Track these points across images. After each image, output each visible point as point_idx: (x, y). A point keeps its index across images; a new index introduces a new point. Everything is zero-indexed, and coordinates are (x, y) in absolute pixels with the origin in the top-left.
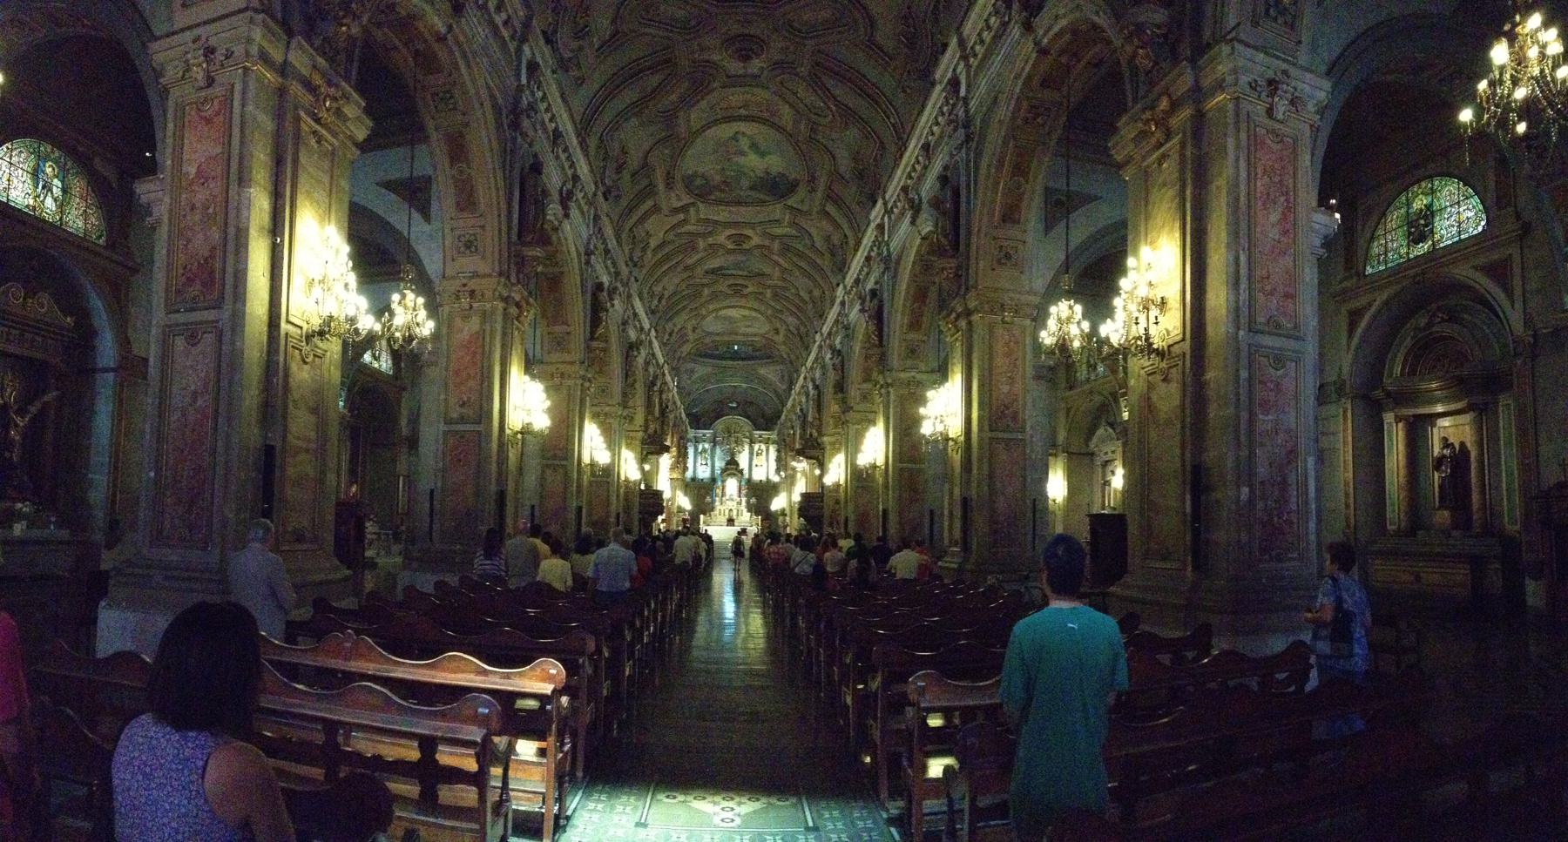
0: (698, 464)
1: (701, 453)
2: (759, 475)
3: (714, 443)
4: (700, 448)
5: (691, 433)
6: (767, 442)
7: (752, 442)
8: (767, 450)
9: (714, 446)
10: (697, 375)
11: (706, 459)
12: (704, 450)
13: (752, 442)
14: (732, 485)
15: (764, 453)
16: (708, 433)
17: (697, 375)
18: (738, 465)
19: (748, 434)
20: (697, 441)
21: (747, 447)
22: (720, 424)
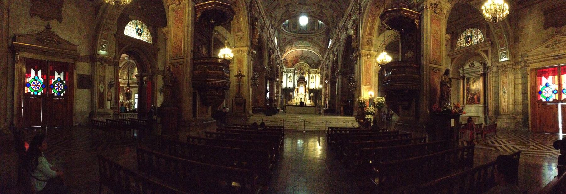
0: (288, 82)
1: (289, 77)
2: (312, 86)
3: (294, 73)
4: (289, 75)
5: (285, 69)
6: (316, 73)
7: (309, 73)
8: (316, 76)
9: (294, 75)
10: (287, 41)
11: (291, 80)
12: (291, 76)
13: (309, 73)
14: (302, 88)
15: (314, 78)
16: (292, 69)
17: (287, 41)
18: (305, 79)
19: (308, 70)
20: (288, 72)
21: (307, 75)
22: (297, 66)
